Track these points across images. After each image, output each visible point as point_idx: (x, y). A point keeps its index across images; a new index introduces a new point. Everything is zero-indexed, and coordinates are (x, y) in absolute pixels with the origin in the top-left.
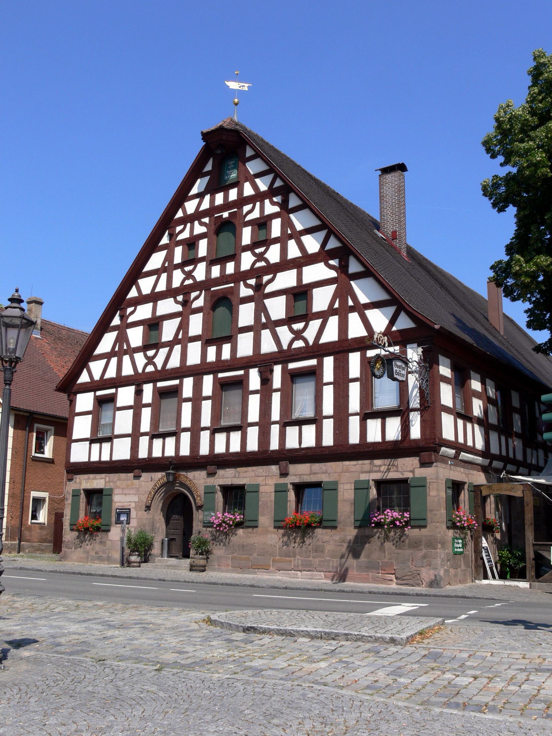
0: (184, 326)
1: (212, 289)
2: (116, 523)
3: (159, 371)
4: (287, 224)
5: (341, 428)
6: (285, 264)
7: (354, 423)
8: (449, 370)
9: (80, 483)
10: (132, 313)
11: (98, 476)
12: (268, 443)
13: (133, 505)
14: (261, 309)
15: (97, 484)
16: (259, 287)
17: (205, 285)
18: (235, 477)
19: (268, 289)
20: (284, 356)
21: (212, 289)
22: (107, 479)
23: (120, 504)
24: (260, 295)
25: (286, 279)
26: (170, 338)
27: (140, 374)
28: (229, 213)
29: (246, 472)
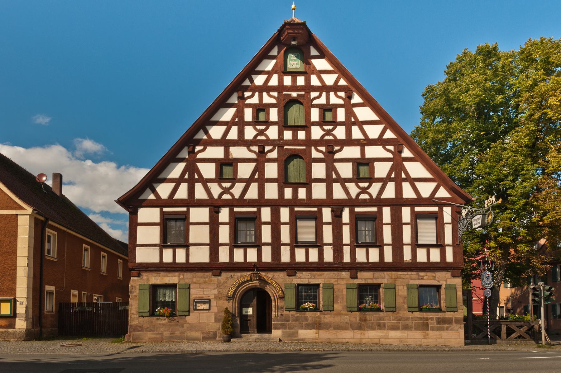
0: (259, 169)
1: (285, 147)
2: (194, 310)
3: (236, 200)
4: (350, 113)
5: (276, 253)
6: (349, 141)
7: (347, 251)
8: (231, 109)
9: (148, 279)
10: (200, 151)
11: (171, 274)
12: (342, 258)
13: (212, 297)
14: (330, 169)
15: (169, 280)
16: (331, 153)
17: (279, 143)
18: (311, 278)
19: (337, 156)
20: (352, 203)
21: (285, 147)
22: (181, 277)
23: (196, 296)
24: (329, 160)
25: (353, 152)
26: (247, 176)
27: (216, 200)
28: (298, 95)
29: (320, 275)
